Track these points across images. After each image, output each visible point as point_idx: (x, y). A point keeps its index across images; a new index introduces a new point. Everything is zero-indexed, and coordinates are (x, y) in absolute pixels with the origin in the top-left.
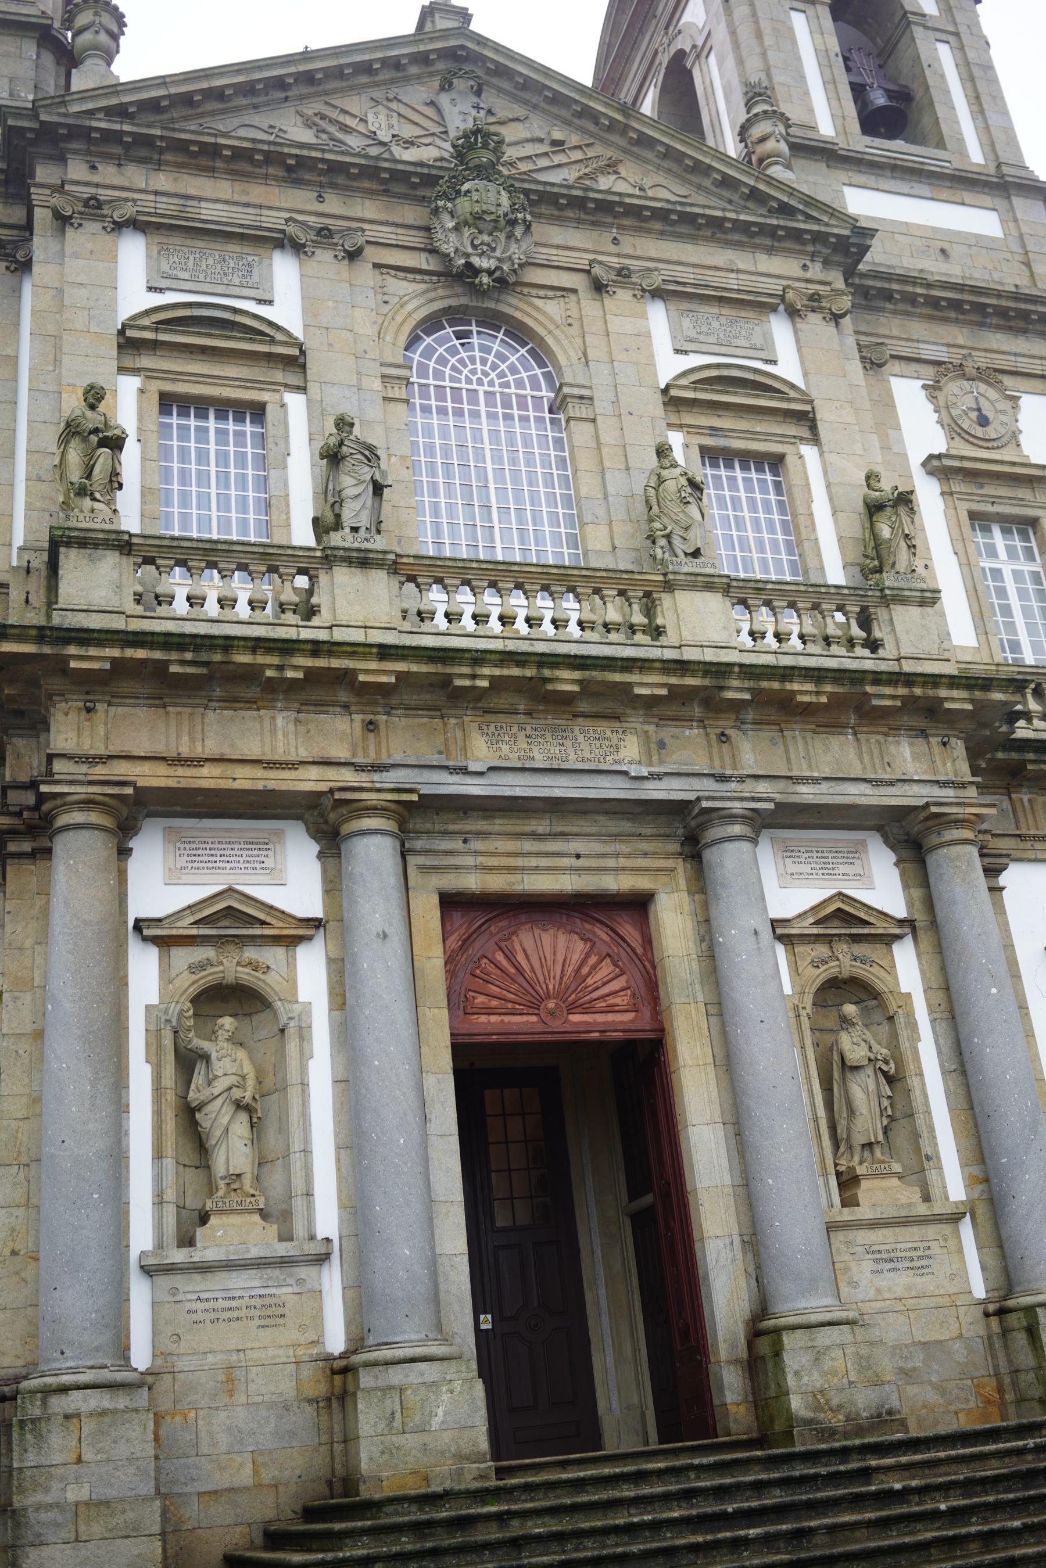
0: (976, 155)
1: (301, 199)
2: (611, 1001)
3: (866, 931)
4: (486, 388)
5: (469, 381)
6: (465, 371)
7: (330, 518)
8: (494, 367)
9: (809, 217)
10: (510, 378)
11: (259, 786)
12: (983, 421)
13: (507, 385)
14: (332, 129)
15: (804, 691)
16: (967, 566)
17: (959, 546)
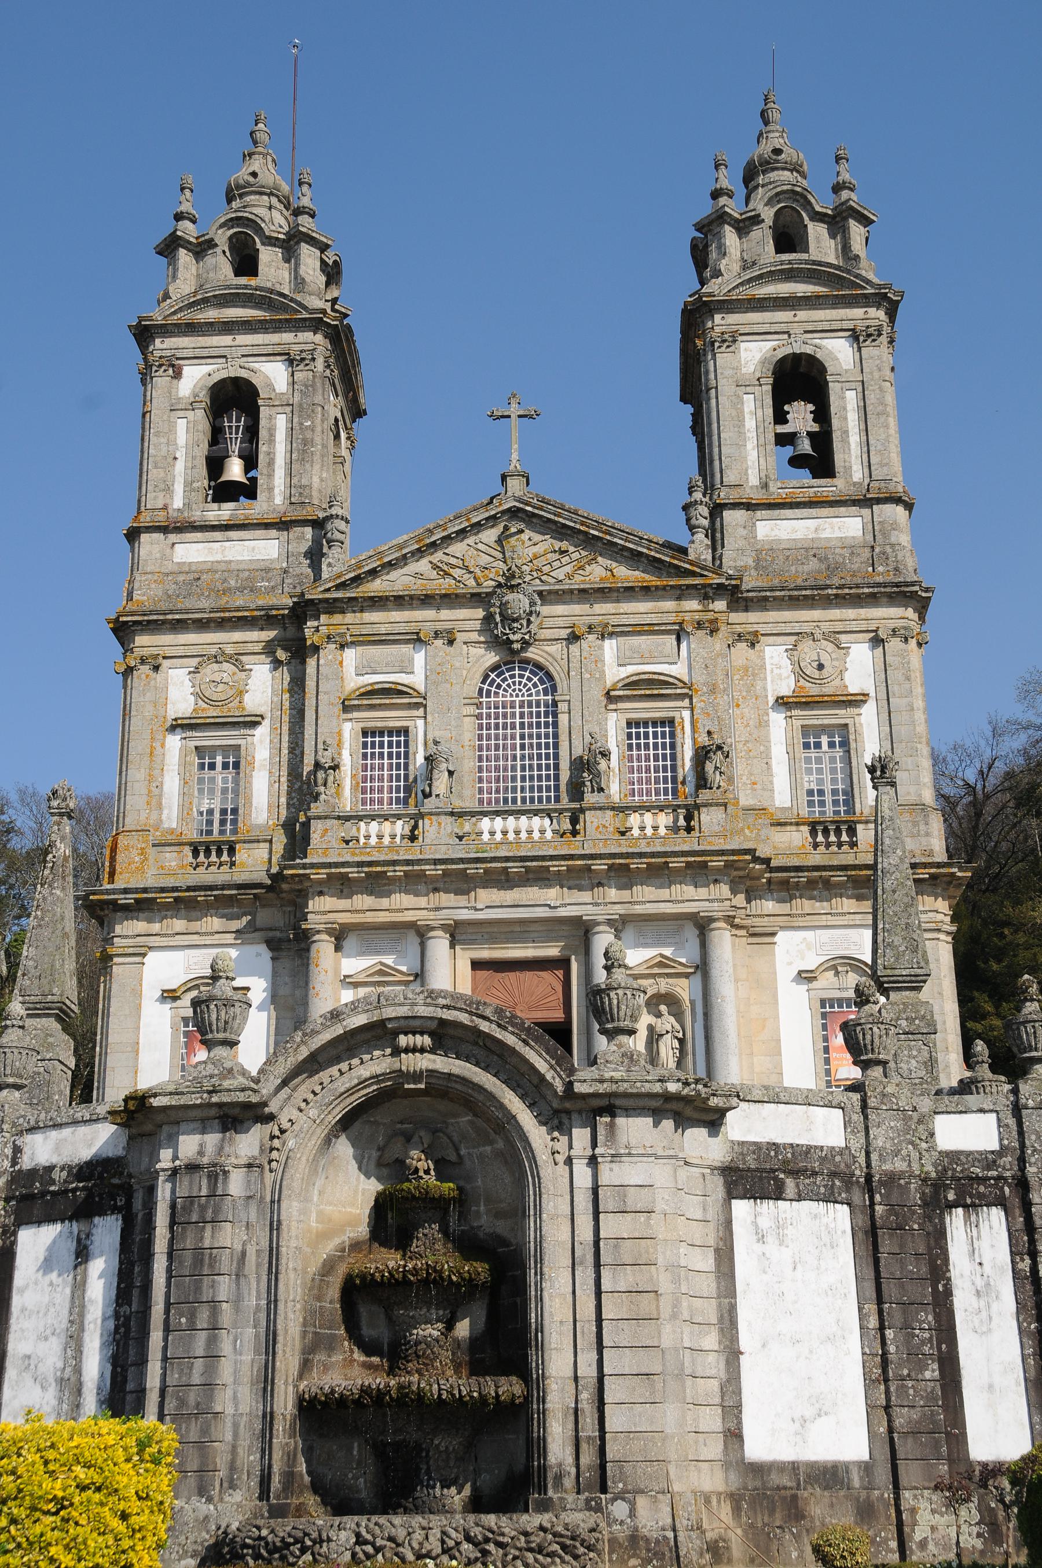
0: (858, 474)
1: (429, 614)
2: (548, 1005)
3: (672, 971)
4: (520, 698)
5: (511, 695)
6: (510, 691)
7: (427, 789)
8: (525, 685)
9: (702, 576)
10: (533, 691)
11: (388, 920)
12: (821, 667)
13: (530, 695)
14: (445, 568)
15: (635, 864)
16: (792, 759)
17: (790, 750)
